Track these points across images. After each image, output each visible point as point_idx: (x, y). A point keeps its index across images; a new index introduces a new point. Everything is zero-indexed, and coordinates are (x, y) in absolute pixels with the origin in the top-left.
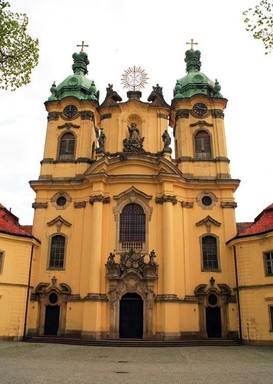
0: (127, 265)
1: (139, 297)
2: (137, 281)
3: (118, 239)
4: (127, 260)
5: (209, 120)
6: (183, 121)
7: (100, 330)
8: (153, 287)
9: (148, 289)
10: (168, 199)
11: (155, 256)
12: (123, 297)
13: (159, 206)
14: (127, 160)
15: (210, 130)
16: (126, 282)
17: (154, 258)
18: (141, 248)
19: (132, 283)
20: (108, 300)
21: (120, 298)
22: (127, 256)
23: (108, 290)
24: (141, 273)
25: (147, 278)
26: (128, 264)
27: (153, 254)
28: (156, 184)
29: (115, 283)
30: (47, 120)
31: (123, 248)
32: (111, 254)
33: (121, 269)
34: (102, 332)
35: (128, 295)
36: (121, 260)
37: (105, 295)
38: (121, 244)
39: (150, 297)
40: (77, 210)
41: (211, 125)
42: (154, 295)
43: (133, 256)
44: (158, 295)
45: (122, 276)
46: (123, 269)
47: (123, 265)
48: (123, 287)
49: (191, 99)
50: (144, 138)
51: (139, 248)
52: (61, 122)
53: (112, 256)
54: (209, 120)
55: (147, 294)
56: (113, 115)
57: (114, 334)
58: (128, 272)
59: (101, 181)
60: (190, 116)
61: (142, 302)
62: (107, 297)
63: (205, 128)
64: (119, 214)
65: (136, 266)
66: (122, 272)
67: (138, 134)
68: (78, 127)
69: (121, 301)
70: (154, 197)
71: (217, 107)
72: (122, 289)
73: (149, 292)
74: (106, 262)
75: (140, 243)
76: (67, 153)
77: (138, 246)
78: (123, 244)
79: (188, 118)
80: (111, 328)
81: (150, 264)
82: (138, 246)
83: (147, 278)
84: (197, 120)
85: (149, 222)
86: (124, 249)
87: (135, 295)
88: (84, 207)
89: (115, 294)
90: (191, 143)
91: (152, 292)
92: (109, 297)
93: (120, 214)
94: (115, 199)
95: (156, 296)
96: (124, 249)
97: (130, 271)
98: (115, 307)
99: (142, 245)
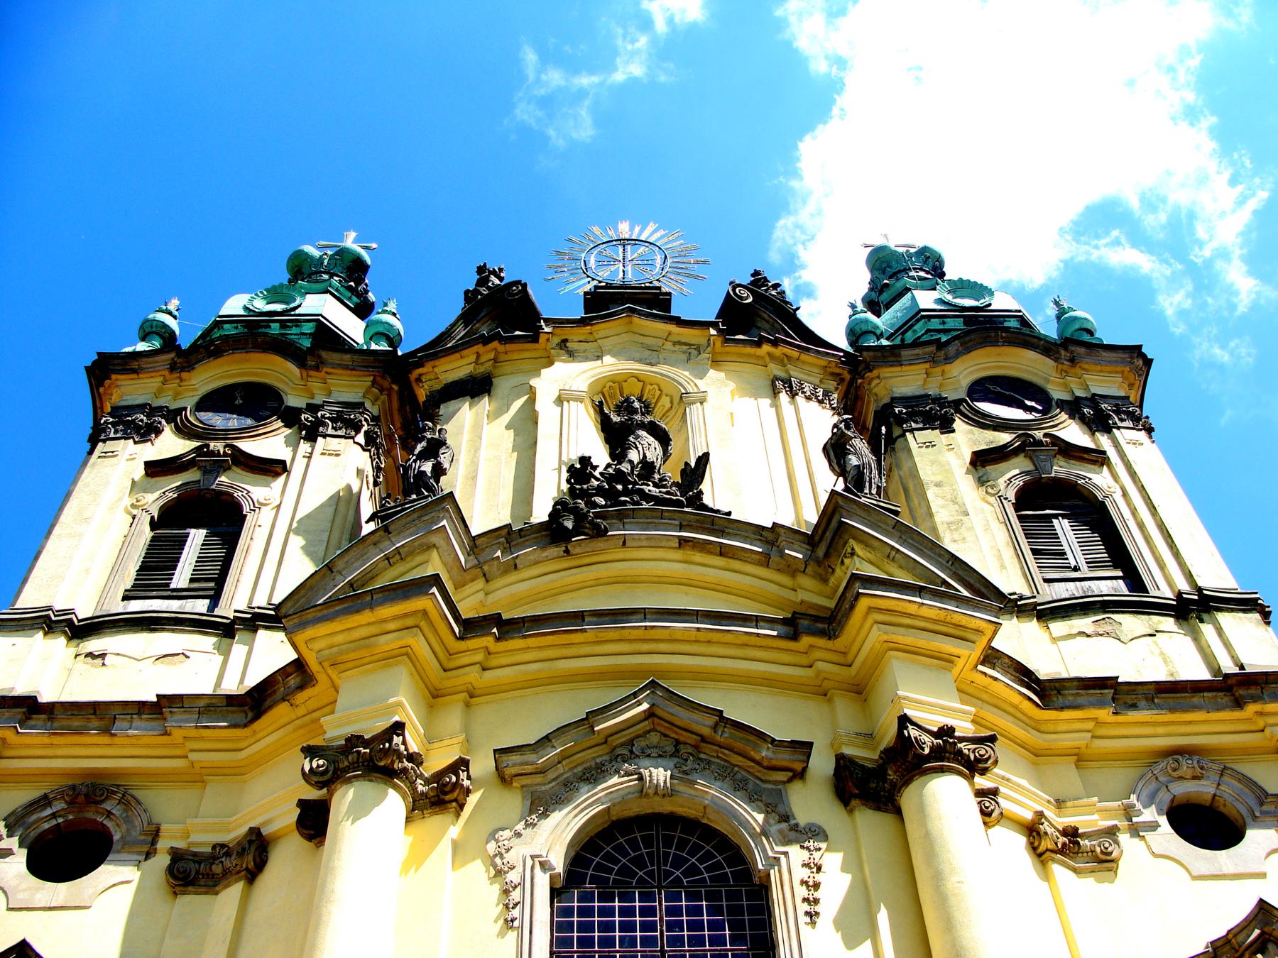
5: (1073, 433)
6: (931, 445)
10: (937, 753)
13: (868, 821)
14: (600, 533)
15: (1100, 480)
28: (822, 693)
30: (88, 446)
40: (191, 902)
41: (1097, 458)
49: (952, 349)
50: (704, 460)
52: (170, 444)
54: (1073, 433)
56: (502, 385)
59: (406, 654)
60: (959, 424)
63: (1061, 469)
64: (543, 884)
67: (666, 455)
68: (271, 468)
70: (821, 764)
71: (1104, 383)
76: (178, 595)
79: (953, 431)
84: (1004, 438)
85: (805, 930)
88: (252, 876)
90: (1001, 535)
93: (555, 893)
94: (503, 778)
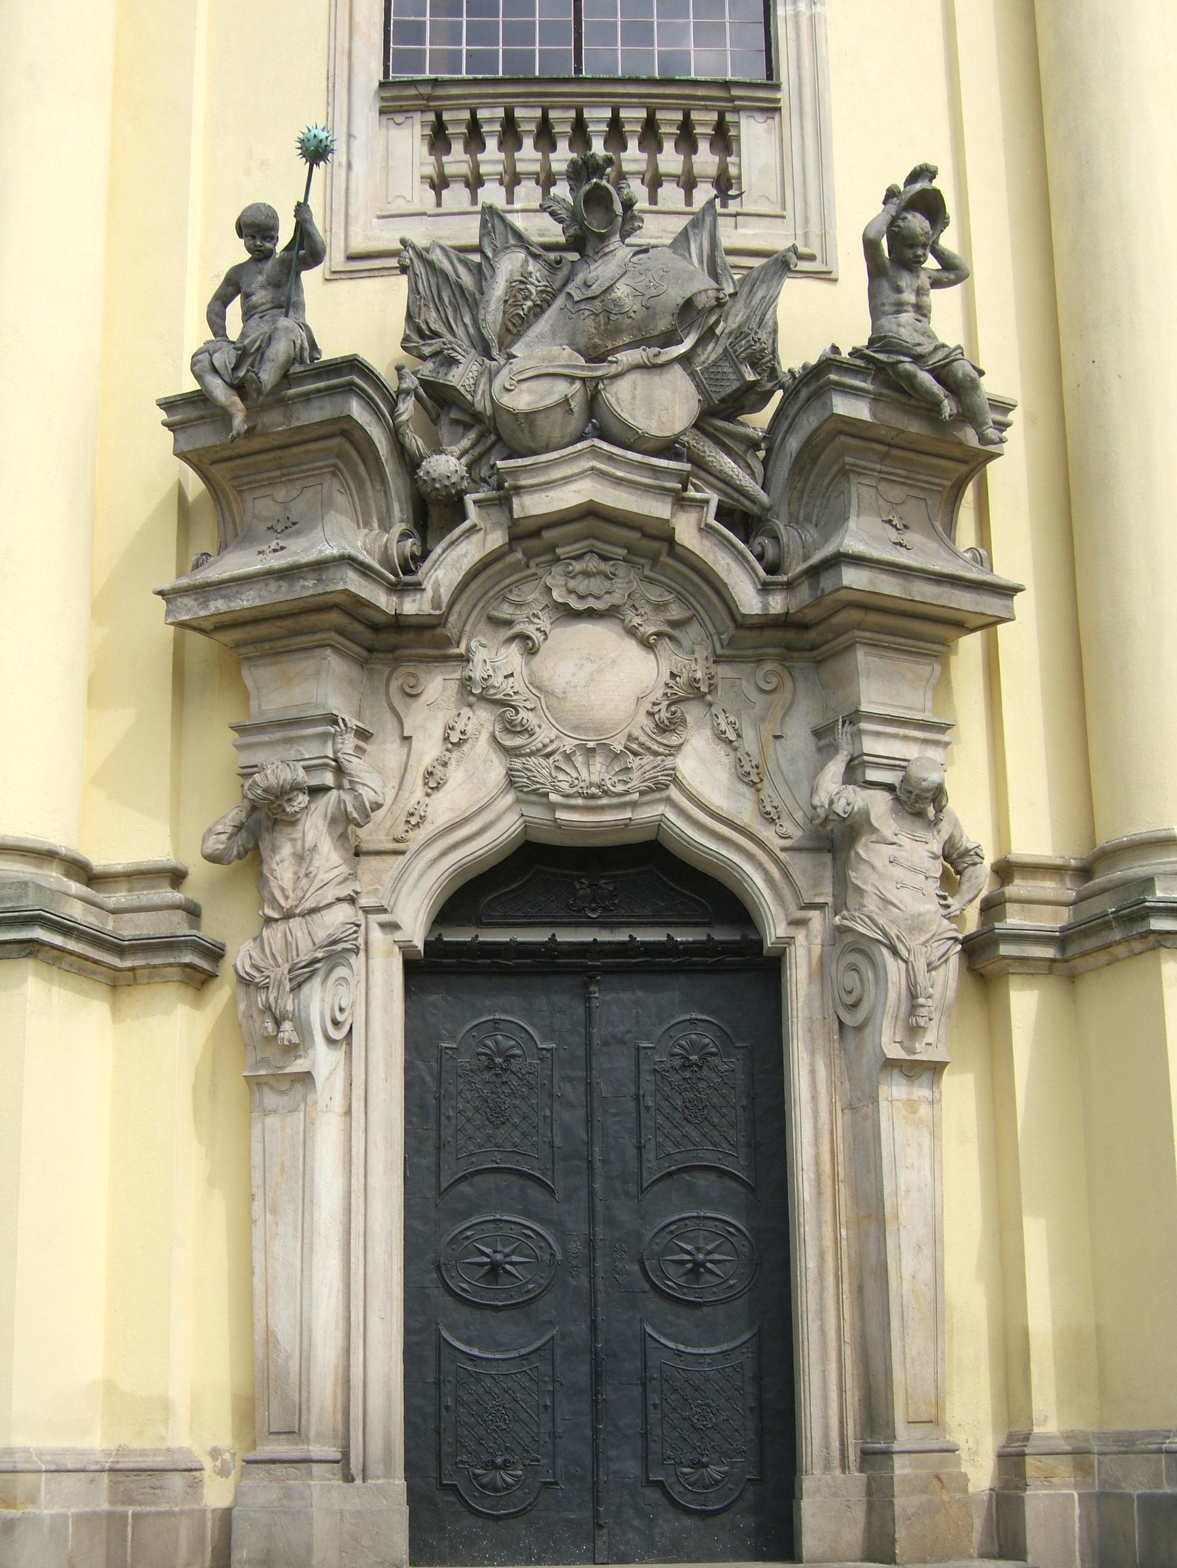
0: (522, 400)
1: (720, 899)
2: (669, 659)
3: (370, 70)
4: (516, 325)
7: (95, 1441)
8: (936, 730)
9: (854, 772)
11: (953, 271)
12: (464, 900)
16: (495, 660)
17: (938, 299)
18: (724, 184)
19: (603, 673)
20: (215, 953)
21: (416, 931)
22: (510, 264)
23: (218, 809)
24: (741, 520)
25: (852, 577)
26: (531, 377)
27: (917, 222)
29: (325, 684)
31: (439, 184)
32: (255, 228)
33: (410, 463)
34: (131, 1477)
35: (531, 873)
36: (417, 333)
37: (177, 877)
38: (409, 140)
39: (898, 873)
42: (955, 860)
43: (600, 272)
44: (1005, 871)
45: (448, 566)
46: (446, 465)
47: (440, 400)
48: (454, 743)
51: (689, 183)
53: (275, 259)
55: (835, 840)
57: (323, 1493)
58: (533, 506)
61: (768, 969)
62: (193, 912)
65: (661, 402)
66: (434, 513)
69: (421, 970)
72: (433, 782)
73: (878, 805)
74: (174, 346)
75: (704, 120)
77: (670, 160)
78: (439, 139)
80: (269, 1407)
81: (883, 365)
82: (670, 160)
83: (852, 577)
86: (456, 196)
87: (652, 871)
89: (329, 859)
91: (920, 802)
92: (228, 923)
95: (981, 880)
96: (456, 196)
97: (561, 488)
98: (323, 1061)
99: (724, 140)
